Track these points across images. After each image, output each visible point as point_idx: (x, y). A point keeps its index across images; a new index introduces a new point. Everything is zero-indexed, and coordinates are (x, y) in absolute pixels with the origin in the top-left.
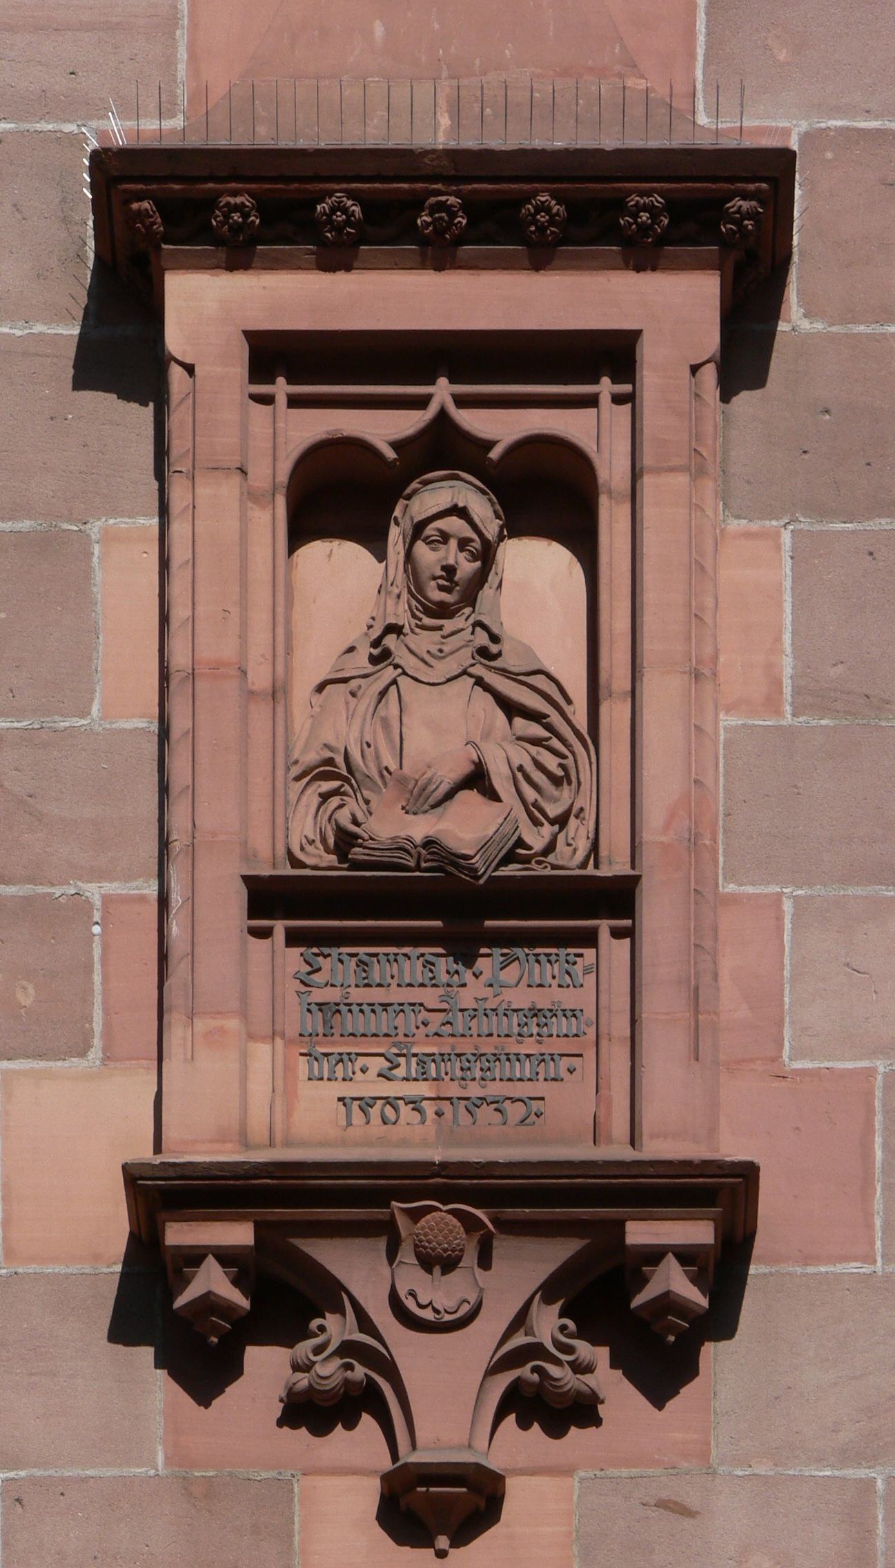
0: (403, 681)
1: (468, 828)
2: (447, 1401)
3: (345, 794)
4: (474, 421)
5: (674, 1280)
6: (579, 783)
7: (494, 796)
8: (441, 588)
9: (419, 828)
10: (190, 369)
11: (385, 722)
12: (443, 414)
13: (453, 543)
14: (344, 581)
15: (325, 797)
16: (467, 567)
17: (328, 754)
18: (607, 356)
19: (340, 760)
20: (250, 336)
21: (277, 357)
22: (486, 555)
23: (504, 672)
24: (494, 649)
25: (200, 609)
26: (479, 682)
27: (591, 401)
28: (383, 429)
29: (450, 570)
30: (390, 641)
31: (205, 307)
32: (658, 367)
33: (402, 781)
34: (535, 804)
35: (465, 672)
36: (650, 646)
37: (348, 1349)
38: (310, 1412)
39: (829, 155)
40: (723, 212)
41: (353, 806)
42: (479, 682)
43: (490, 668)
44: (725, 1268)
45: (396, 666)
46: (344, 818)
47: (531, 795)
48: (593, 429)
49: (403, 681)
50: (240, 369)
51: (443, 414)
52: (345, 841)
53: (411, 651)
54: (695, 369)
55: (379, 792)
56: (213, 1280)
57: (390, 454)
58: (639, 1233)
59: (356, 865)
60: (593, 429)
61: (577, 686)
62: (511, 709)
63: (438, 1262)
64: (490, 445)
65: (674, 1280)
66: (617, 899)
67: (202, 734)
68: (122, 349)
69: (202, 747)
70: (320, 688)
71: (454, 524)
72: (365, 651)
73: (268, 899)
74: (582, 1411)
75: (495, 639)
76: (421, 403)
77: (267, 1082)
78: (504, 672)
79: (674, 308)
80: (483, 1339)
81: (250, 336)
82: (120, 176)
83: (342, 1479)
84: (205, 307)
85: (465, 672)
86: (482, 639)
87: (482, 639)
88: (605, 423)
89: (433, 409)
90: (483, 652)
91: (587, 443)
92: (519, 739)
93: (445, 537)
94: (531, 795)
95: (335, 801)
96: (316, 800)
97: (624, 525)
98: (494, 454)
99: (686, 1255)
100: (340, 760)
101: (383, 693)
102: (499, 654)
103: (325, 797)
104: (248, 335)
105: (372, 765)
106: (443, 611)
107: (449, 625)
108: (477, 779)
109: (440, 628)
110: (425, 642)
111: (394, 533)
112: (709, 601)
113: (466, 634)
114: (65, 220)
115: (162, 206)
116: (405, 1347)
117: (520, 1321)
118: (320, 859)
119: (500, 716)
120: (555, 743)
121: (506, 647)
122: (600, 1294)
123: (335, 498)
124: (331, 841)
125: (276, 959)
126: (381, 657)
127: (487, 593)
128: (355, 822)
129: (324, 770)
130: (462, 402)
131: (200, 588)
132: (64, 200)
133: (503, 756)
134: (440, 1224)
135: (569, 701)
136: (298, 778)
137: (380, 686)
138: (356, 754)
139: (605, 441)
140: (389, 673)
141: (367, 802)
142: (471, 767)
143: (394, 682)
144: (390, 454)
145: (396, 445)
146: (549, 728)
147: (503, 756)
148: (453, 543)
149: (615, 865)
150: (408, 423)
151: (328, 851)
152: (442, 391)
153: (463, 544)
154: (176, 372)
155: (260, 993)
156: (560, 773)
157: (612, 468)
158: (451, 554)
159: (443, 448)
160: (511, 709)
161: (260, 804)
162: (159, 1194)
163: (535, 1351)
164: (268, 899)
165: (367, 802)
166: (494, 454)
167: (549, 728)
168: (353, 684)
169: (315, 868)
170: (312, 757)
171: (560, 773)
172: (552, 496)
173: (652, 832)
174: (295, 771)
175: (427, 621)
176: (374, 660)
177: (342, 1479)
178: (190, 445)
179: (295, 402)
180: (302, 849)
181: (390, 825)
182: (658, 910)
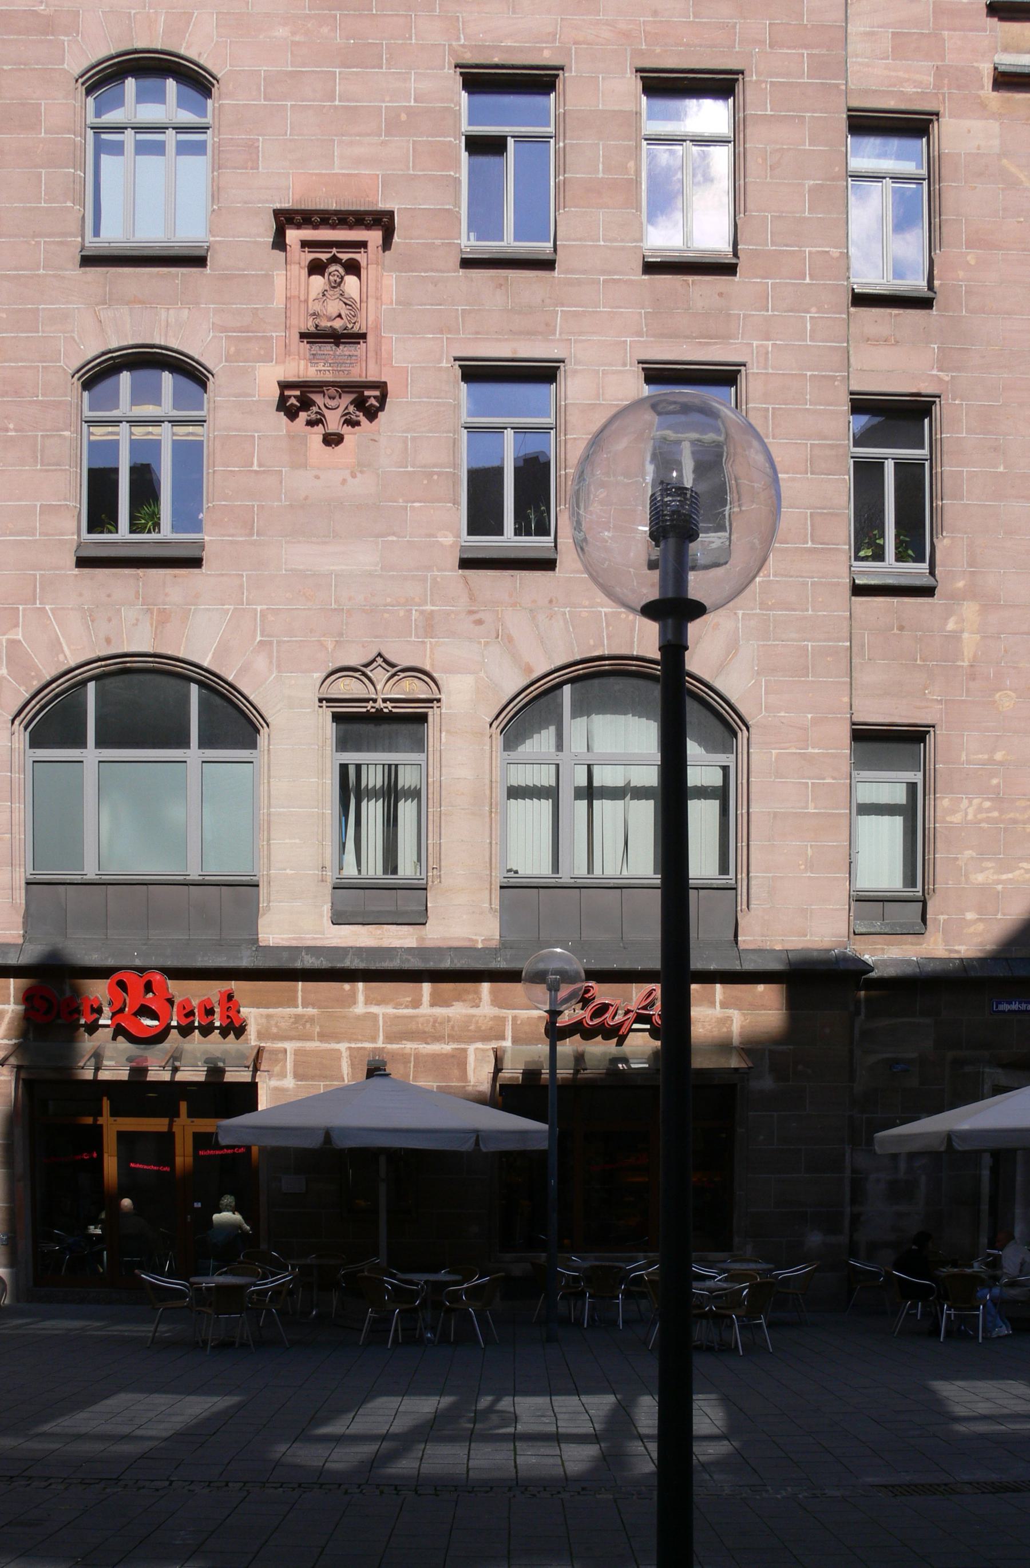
1: (338, 324)
2: (334, 422)
4: (339, 255)
5: (373, 401)
9: (329, 324)
14: (318, 282)
16: (338, 280)
18: (363, 245)
21: (305, 244)
22: (342, 278)
28: (324, 257)
31: (293, 236)
37: (317, 413)
38: (310, 423)
44: (383, 399)
48: (360, 257)
56: (293, 401)
58: (366, 393)
60: (360, 257)
61: (358, 301)
62: (346, 304)
63: (332, 398)
65: (373, 401)
66: (363, 336)
68: (279, 243)
74: (357, 424)
77: (304, 366)
79: (374, 237)
80: (340, 411)
82: (277, 213)
83: (316, 435)
84: (293, 236)
99: (375, 397)
106: (334, 287)
108: (340, 316)
110: (331, 293)
115: (286, 219)
116: (326, 412)
117: (346, 408)
118: (313, 329)
122: (360, 403)
123: (316, 268)
125: (304, 346)
126: (324, 295)
129: (314, 314)
134: (332, 391)
149: (365, 331)
150: (329, 256)
152: (334, 250)
155: (302, 351)
157: (363, 264)
159: (334, 260)
160: (346, 304)
161: (302, 319)
162: (284, 386)
163: (349, 413)
164: (303, 336)
172: (353, 268)
173: (370, 323)
177: (316, 435)
181: (325, 324)
182: (370, 338)
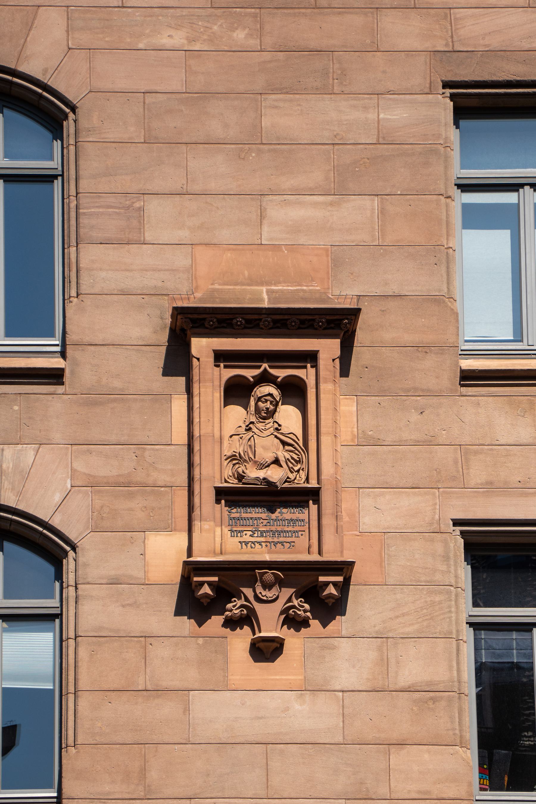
0: (255, 436)
3: (240, 464)
4: (273, 371)
6: (303, 462)
7: (281, 466)
8: (265, 413)
9: (261, 474)
10: (198, 359)
11: (250, 446)
12: (265, 369)
13: (269, 402)
15: (234, 465)
17: (235, 453)
18: (311, 358)
19: (237, 455)
20: (214, 351)
21: (221, 357)
22: (276, 405)
23: (282, 434)
24: (279, 428)
25: (202, 419)
26: (276, 437)
27: (305, 367)
28: (250, 374)
29: (267, 409)
30: (251, 426)
31: (201, 346)
32: (324, 360)
33: (256, 462)
34: (292, 468)
35: (272, 434)
36: (323, 430)
39: (366, 304)
40: (340, 323)
41: (243, 468)
42: (276, 437)
43: (278, 433)
45: (253, 432)
46: (240, 470)
47: (291, 465)
48: (307, 374)
49: (255, 436)
50: (212, 360)
51: (265, 369)
52: (240, 477)
53: (257, 428)
54: (333, 360)
55: (248, 463)
57: (252, 380)
59: (244, 484)
60: (307, 374)
61: (300, 437)
62: (284, 443)
64: (278, 377)
67: (202, 451)
69: (203, 453)
70: (231, 436)
71: (269, 398)
72: (244, 427)
73: (222, 494)
75: (280, 425)
76: (259, 367)
78: (282, 434)
79: (328, 348)
81: (214, 351)
82: (179, 312)
84: (201, 346)
85: (272, 434)
86: (276, 426)
87: (276, 426)
88: (309, 372)
89: (262, 369)
90: (277, 429)
91: (304, 378)
92: (286, 451)
93: (266, 401)
94: (291, 465)
95: (237, 466)
96: (232, 466)
97: (314, 397)
98: (279, 380)
100: (237, 455)
101: (249, 439)
102: (280, 430)
103: (234, 465)
104: (213, 350)
105: (247, 457)
106: (265, 418)
107: (267, 421)
108: (276, 462)
109: (265, 422)
110: (260, 426)
111: (252, 399)
112: (338, 418)
113: (271, 424)
114: (162, 318)
118: (233, 483)
119: (281, 446)
120: (296, 452)
121: (282, 428)
123: (236, 392)
124: (236, 476)
126: (248, 429)
127: (277, 414)
128: (243, 472)
129: (232, 458)
130: (271, 367)
131: (202, 414)
132: (161, 313)
133: (282, 454)
135: (299, 440)
136: (226, 460)
137: (249, 437)
138: (242, 454)
139: (308, 377)
140: (251, 434)
141: (245, 466)
142: (274, 459)
143: (253, 436)
144: (252, 380)
145: (253, 377)
146: (295, 448)
147: (282, 454)
148: (269, 402)
150: (256, 372)
151: (235, 478)
152: (265, 365)
153: (271, 403)
154: (195, 360)
156: (298, 459)
157: (311, 382)
158: (268, 405)
159: (265, 378)
160: (284, 443)
161: (217, 468)
164: (222, 494)
165: (245, 466)
166: (279, 380)
167: (295, 448)
168: (241, 436)
169: (233, 483)
170: (229, 454)
171: (298, 459)
172: (294, 392)
174: (225, 457)
175: (261, 420)
176: (246, 430)
178: (198, 378)
179: (226, 367)
180: (228, 478)
181: (253, 473)
